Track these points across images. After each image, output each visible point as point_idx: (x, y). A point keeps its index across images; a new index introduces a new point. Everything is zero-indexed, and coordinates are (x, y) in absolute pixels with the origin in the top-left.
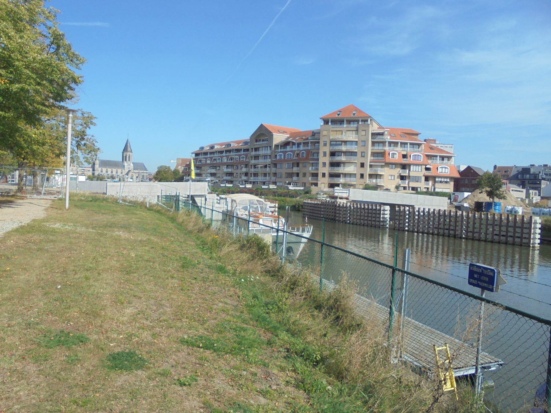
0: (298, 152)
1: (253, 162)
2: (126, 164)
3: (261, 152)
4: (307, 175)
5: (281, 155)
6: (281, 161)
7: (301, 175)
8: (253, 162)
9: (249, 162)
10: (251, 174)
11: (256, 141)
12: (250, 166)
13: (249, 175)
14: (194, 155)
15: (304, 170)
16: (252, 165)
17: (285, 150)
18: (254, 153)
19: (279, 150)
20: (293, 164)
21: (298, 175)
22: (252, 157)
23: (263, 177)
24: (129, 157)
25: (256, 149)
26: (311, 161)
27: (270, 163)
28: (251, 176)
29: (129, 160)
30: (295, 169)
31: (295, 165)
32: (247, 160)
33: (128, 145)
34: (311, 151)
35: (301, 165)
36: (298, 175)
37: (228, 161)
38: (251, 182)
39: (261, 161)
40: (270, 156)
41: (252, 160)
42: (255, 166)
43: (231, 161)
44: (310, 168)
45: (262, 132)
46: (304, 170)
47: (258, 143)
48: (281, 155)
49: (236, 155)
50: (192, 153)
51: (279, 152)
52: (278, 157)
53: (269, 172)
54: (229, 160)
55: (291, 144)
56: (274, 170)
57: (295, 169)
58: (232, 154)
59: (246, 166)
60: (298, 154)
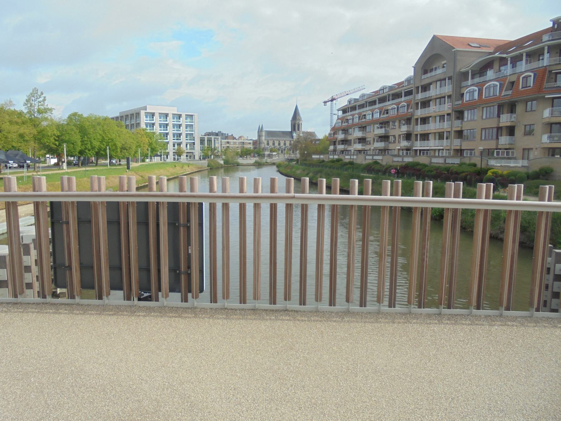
0: (514, 78)
1: (420, 113)
2: (294, 135)
3: (433, 92)
4: (538, 129)
5: (474, 91)
6: (472, 106)
7: (519, 132)
8: (420, 113)
9: (412, 115)
10: (417, 135)
11: (425, 72)
12: (413, 121)
13: (413, 137)
14: (340, 113)
15: (528, 119)
16: (417, 119)
17: (482, 79)
18: (420, 96)
19: (470, 82)
20: (500, 107)
21: (511, 130)
22: (417, 104)
23: (437, 141)
24: (299, 126)
25: (425, 88)
26: (550, 94)
27: (450, 111)
28: (416, 140)
29: (299, 130)
30: (506, 120)
31: (506, 109)
32: (410, 111)
33: (297, 112)
34: (548, 69)
35: (519, 108)
36: (511, 130)
37: (382, 116)
38: (416, 150)
39: (433, 109)
40: (449, 97)
41: (417, 109)
42: (425, 120)
43: (386, 116)
44: (547, 113)
45: (435, 53)
46: (528, 119)
47: (429, 75)
48: (474, 91)
49: (392, 104)
50: (338, 110)
51: (467, 86)
52: (467, 97)
53: (449, 130)
54: (384, 114)
55: (496, 65)
56: (457, 125)
57: (506, 120)
58: (387, 103)
59: (408, 121)
60: (513, 83)
